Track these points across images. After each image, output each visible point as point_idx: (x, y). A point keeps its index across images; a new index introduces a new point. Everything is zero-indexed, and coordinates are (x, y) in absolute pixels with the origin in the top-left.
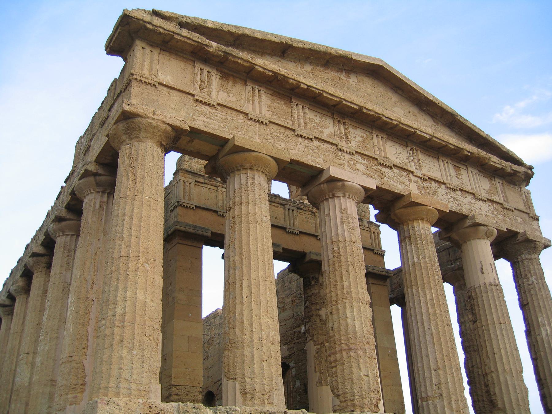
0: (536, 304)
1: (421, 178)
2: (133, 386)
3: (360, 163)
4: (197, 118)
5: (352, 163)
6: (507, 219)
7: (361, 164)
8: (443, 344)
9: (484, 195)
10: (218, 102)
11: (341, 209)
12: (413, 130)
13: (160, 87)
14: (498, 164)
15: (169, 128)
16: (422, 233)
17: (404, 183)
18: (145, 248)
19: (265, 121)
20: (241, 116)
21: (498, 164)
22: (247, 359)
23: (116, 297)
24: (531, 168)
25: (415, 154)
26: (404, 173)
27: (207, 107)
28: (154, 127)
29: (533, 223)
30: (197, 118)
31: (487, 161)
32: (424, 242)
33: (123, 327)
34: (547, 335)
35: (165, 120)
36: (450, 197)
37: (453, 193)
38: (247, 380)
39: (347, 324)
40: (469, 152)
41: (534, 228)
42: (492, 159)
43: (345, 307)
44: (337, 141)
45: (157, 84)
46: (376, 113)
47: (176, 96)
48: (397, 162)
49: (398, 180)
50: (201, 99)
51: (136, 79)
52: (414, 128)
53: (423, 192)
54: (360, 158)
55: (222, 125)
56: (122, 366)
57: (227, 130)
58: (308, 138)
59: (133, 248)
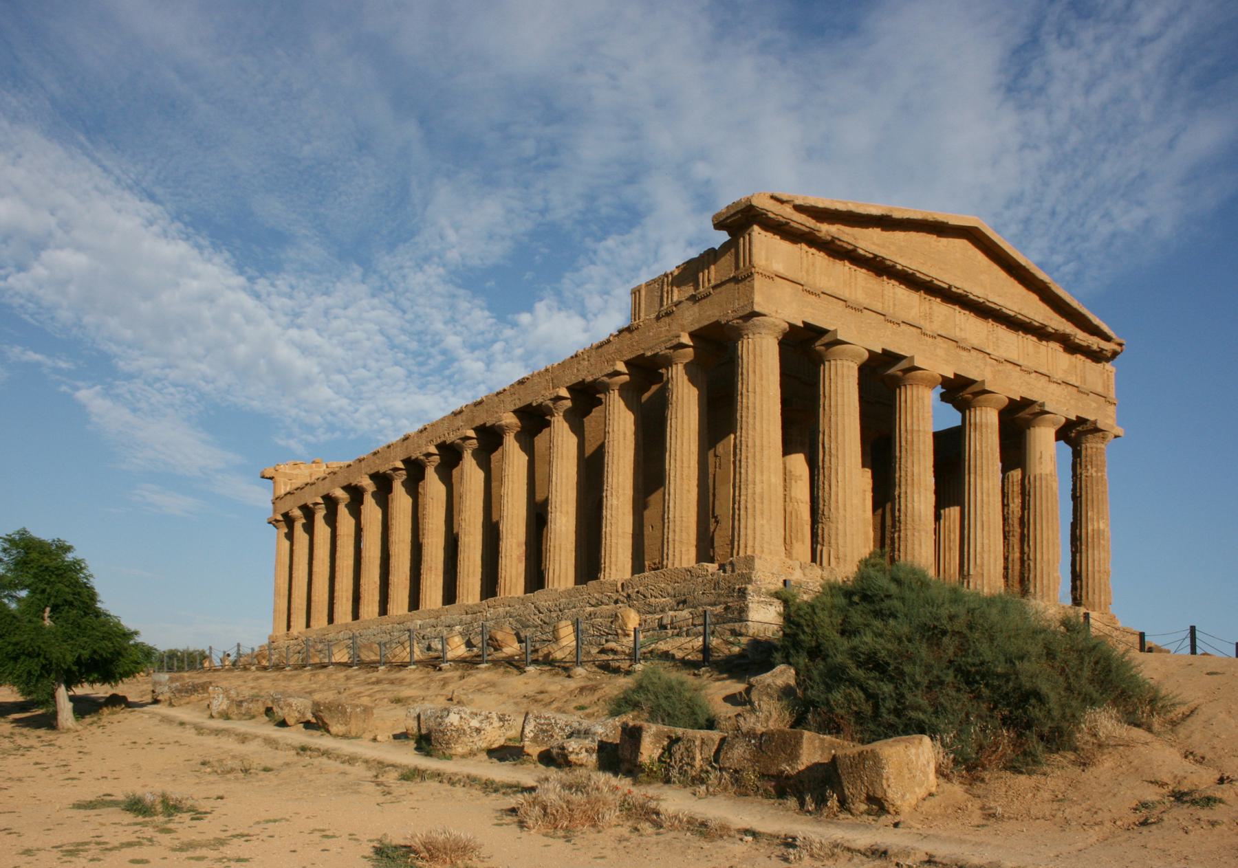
0: (1089, 497)
13: (776, 278)
16: (989, 421)
26: (981, 355)
27: (814, 297)
32: (989, 431)
34: (1093, 530)
37: (1026, 377)
39: (913, 507)
43: (913, 493)
44: (922, 323)
45: (773, 276)
48: (975, 342)
50: (809, 289)
54: (941, 341)
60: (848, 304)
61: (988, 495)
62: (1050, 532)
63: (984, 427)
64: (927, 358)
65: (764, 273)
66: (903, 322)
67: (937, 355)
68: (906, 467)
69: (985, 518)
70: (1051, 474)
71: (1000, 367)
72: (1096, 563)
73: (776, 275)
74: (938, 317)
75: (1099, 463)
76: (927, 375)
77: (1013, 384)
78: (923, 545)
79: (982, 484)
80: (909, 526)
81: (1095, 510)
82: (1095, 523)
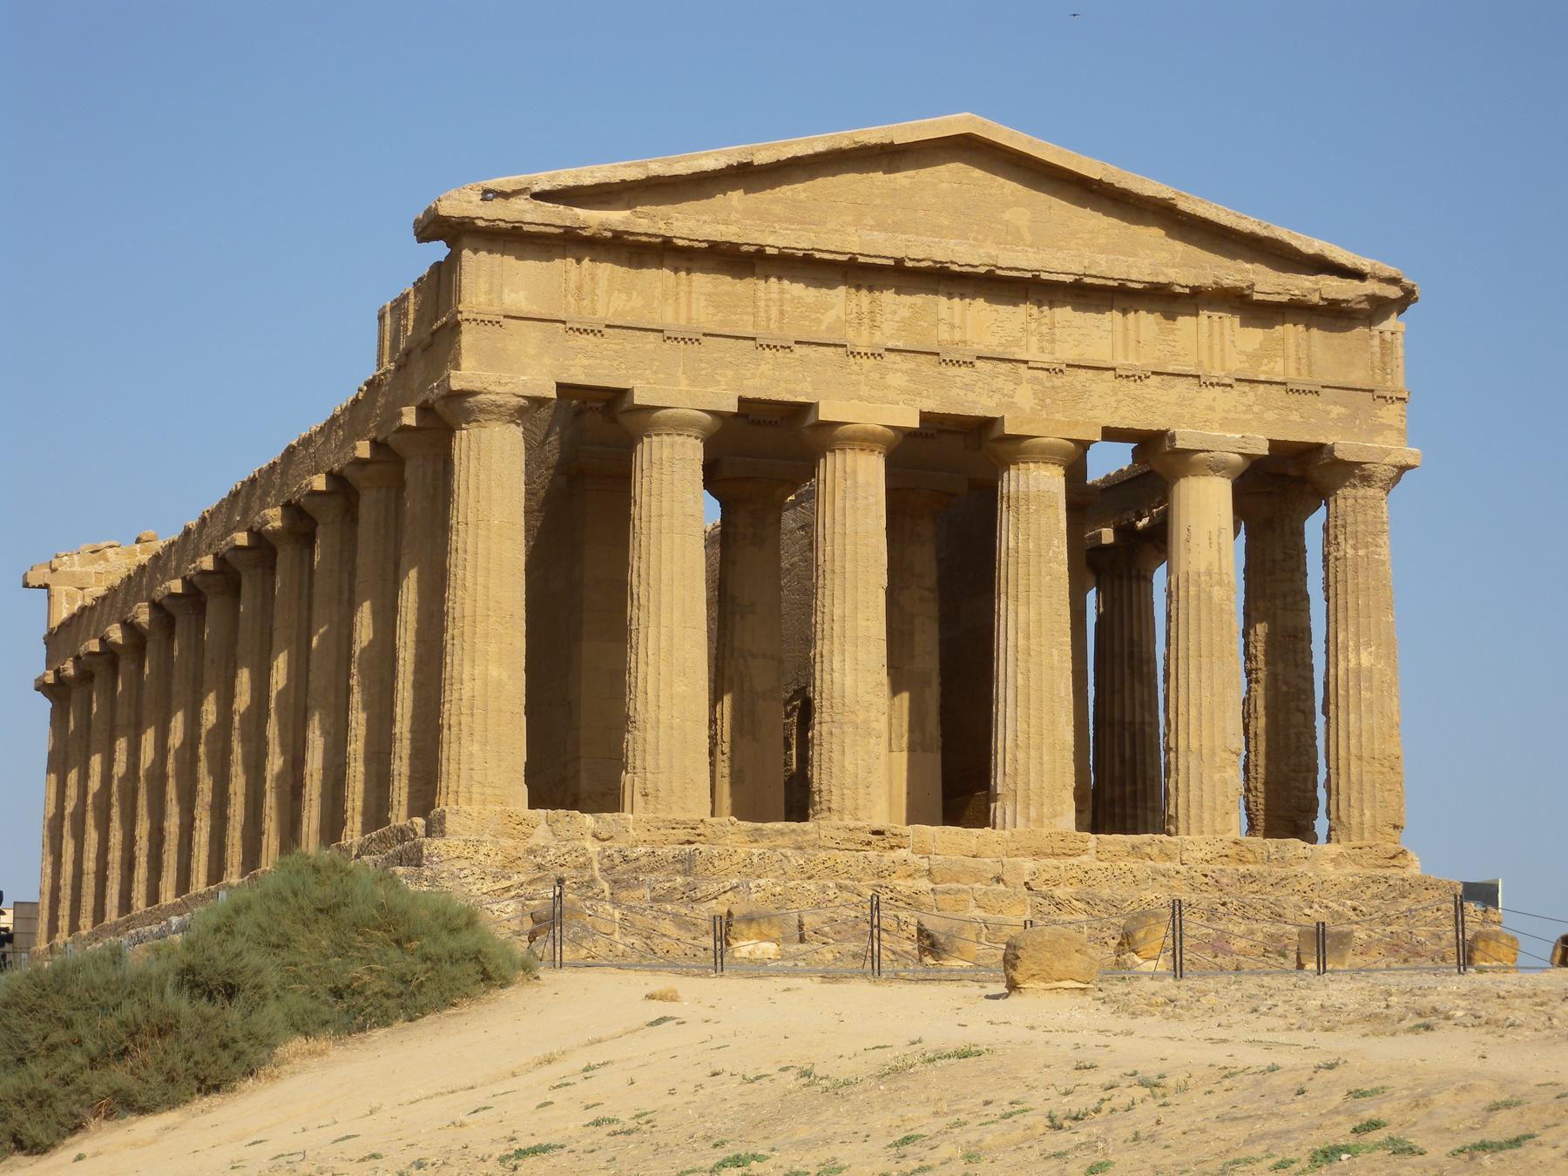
1: (1048, 370)
2: (488, 791)
3: (900, 371)
4: (571, 362)
5: (875, 375)
6: (1295, 417)
7: (898, 372)
8: (1033, 705)
10: (607, 323)
11: (845, 472)
12: (1029, 275)
14: (1279, 294)
15: (523, 401)
16: (1033, 489)
17: (999, 390)
18: (497, 602)
19: (694, 337)
20: (652, 335)
21: (1279, 294)
22: (650, 748)
23: (461, 673)
24: (1394, 281)
25: (1045, 313)
28: (501, 406)
29: (1379, 413)
30: (571, 362)
31: (1247, 292)
33: (472, 715)
35: (516, 391)
36: (1121, 396)
40: (1187, 286)
41: (1383, 425)
42: (1256, 288)
43: (832, 652)
47: (533, 332)
49: (986, 386)
50: (576, 326)
52: (1032, 271)
53: (1048, 401)
55: (616, 363)
56: (473, 767)
57: (624, 372)
58: (781, 347)
59: (480, 603)
60: (667, 334)
61: (1028, 638)
62: (1206, 693)
63: (1022, 502)
64: (860, 398)
65: (480, 317)
66: (797, 342)
67: (887, 387)
68: (824, 606)
69: (1020, 681)
70: (1209, 573)
71: (1058, 381)
72: (1353, 742)
75: (1361, 528)
76: (854, 432)
79: (1017, 613)
80: (826, 717)
81: (1352, 629)
82: (1352, 656)
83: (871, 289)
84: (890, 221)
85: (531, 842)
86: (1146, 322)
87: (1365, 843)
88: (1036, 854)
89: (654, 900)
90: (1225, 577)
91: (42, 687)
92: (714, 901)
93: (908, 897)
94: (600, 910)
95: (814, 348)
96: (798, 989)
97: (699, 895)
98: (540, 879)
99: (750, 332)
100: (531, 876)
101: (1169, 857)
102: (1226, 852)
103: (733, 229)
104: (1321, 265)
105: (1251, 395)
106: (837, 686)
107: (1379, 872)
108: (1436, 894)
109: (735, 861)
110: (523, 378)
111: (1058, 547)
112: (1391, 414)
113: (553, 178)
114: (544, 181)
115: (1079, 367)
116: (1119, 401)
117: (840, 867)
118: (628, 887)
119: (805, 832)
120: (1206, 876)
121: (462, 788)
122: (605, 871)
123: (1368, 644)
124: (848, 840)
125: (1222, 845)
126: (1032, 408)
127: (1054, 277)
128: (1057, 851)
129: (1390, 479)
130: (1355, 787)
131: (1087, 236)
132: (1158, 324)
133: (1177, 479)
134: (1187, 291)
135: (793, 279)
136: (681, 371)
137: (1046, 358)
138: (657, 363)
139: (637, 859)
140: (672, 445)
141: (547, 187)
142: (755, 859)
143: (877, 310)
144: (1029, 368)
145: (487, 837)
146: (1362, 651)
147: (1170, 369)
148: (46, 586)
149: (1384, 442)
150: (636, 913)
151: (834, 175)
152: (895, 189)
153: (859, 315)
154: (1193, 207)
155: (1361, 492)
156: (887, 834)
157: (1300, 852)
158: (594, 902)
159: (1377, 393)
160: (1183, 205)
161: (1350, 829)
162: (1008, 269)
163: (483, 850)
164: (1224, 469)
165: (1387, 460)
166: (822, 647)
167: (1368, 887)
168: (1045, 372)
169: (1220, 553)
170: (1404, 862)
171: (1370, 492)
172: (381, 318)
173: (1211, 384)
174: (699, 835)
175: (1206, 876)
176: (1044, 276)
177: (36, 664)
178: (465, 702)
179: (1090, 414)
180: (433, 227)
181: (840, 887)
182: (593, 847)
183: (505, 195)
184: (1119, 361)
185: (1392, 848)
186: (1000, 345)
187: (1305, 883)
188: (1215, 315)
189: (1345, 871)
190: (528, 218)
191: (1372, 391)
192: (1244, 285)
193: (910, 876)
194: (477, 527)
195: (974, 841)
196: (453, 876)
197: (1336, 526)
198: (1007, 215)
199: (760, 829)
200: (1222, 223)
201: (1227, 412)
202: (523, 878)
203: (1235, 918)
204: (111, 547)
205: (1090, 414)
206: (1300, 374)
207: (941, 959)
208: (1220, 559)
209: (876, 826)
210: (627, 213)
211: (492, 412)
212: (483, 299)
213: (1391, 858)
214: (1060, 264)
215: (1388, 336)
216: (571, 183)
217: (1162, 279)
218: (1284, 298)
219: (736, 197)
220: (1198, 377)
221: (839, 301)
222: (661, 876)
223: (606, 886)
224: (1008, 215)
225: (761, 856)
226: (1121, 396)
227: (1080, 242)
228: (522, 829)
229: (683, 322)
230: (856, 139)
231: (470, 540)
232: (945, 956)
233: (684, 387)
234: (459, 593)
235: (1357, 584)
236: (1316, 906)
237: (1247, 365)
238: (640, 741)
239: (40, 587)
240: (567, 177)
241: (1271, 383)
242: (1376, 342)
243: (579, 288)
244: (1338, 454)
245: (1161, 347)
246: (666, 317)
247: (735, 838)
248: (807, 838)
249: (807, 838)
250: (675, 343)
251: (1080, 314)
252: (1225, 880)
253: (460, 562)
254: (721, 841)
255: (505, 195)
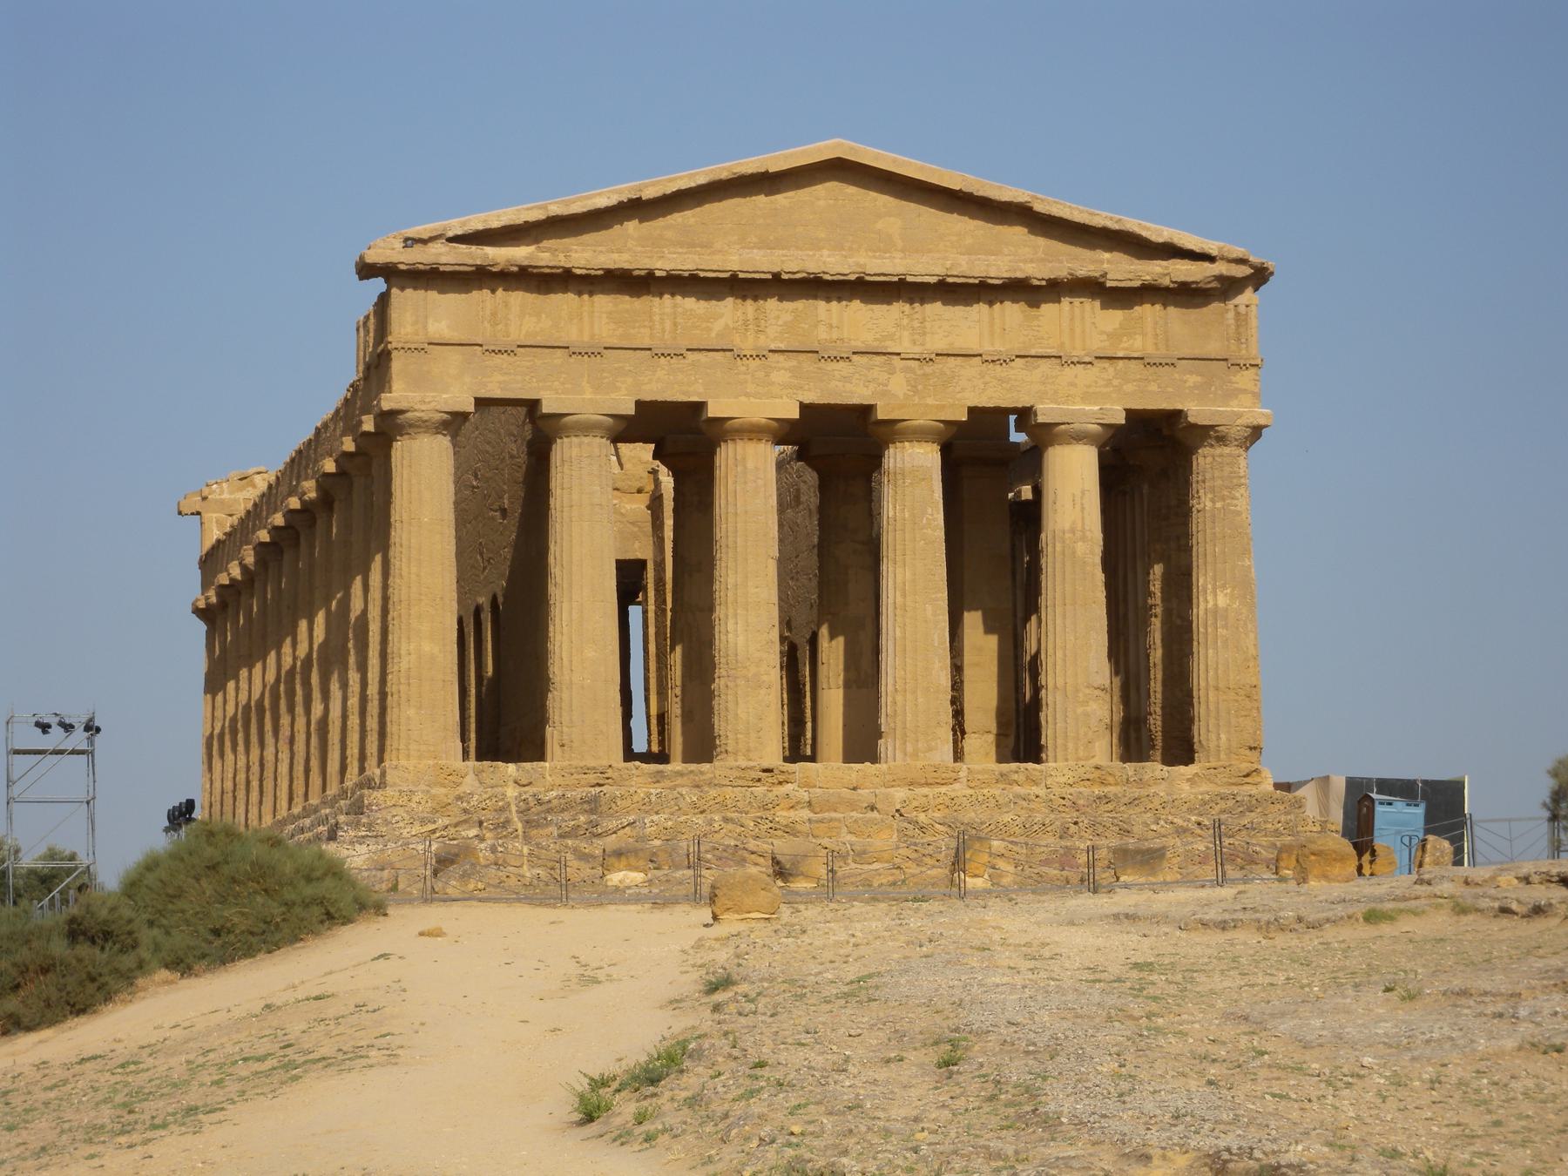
2: (423, 748)
3: (783, 368)
5: (761, 374)
6: (1153, 387)
7: (782, 371)
9: (1098, 344)
12: (896, 279)
15: (446, 416)
23: (399, 649)
24: (1242, 261)
28: (426, 421)
29: (1234, 379)
31: (1102, 280)
33: (409, 684)
35: (438, 408)
36: (987, 378)
38: (565, 729)
40: (1043, 279)
41: (1237, 389)
42: (1108, 277)
46: (808, 273)
47: (454, 355)
50: (492, 348)
51: (396, 349)
53: (920, 387)
60: (572, 350)
63: (899, 477)
64: (747, 395)
65: (407, 346)
66: (688, 350)
69: (898, 633)
70: (1073, 531)
71: (928, 369)
72: (1211, 673)
73: (429, 344)
74: (778, 317)
77: (963, 390)
78: (740, 701)
81: (1210, 574)
82: (1210, 598)
83: (755, 299)
84: (771, 238)
85: (460, 791)
86: (1011, 312)
87: (1221, 763)
88: (912, 784)
89: (560, 836)
90: (1088, 534)
91: (198, 612)
92: (614, 835)
93: (786, 826)
94: (510, 847)
95: (705, 353)
96: (561, 922)
97: (600, 831)
98: (465, 821)
99: (646, 343)
100: (458, 819)
101: (1036, 783)
102: (1086, 776)
103: (626, 256)
104: (1171, 251)
105: (1111, 370)
106: (731, 645)
107: (1225, 790)
108: (1282, 808)
109: (635, 800)
110: (444, 396)
111: (932, 515)
112: (1244, 379)
113: (464, 224)
114: (456, 227)
115: (948, 355)
116: (986, 383)
117: (728, 802)
118: (538, 826)
119: (702, 773)
120: (1064, 798)
121: (402, 747)
122: (521, 812)
123: (1224, 587)
124: (740, 778)
125: (1083, 770)
126: (905, 394)
127: (919, 279)
128: (930, 781)
129: (1246, 438)
130: (1213, 714)
131: (954, 238)
132: (1022, 312)
133: (1047, 447)
134: (1044, 283)
135: (684, 295)
136: (585, 379)
137: (917, 349)
138: (564, 376)
139: (550, 801)
140: (580, 445)
141: (460, 232)
142: (653, 798)
143: (761, 317)
144: (902, 359)
145: (423, 787)
146: (1219, 593)
147: (1033, 352)
148: (199, 513)
149: (1238, 406)
150: (542, 848)
151: (720, 201)
152: (776, 209)
153: (746, 323)
154: (1047, 208)
155: (1218, 451)
156: (776, 771)
157: (1158, 774)
158: (504, 840)
159: (1230, 362)
160: (1039, 207)
161: (1208, 751)
162: (875, 275)
163: (416, 799)
164: (1085, 438)
165: (1239, 422)
166: (720, 612)
167: (1217, 804)
168: (917, 362)
169: (1083, 512)
170: (1257, 779)
171: (1227, 450)
172: (358, 330)
173: (1072, 363)
174: (608, 778)
175: (1064, 798)
176: (910, 279)
177: (190, 588)
178: (403, 674)
179: (958, 396)
180: (367, 271)
181: (726, 820)
182: (512, 792)
183: (424, 242)
184: (986, 348)
185: (1245, 767)
186: (876, 340)
187: (1157, 802)
188: (1077, 301)
189: (1201, 789)
190: (443, 260)
191: (1226, 360)
192: (1097, 275)
193: (792, 807)
194: (410, 524)
195: (854, 775)
196: (387, 823)
197: (1198, 482)
198: (879, 225)
199: (662, 772)
200: (1076, 220)
201: (1090, 386)
202: (447, 821)
203: (1086, 835)
204: (259, 473)
205: (958, 396)
206: (1157, 349)
207: (788, 881)
208: (1083, 518)
209: (766, 765)
210: (532, 249)
211: (419, 427)
212: (409, 329)
213: (1244, 776)
214: (924, 268)
215: (1242, 309)
216: (480, 227)
217: (1019, 275)
218: (1137, 284)
219: (632, 226)
220: (1060, 357)
221: (728, 311)
222: (566, 815)
223: (520, 826)
224: (879, 225)
225: (659, 795)
226: (987, 378)
227: (948, 244)
228: (454, 777)
229: (586, 338)
230: (735, 171)
231: (405, 536)
232: (791, 879)
233: (588, 396)
234: (398, 581)
235: (1214, 533)
236: (1162, 822)
237: (1107, 343)
238: (557, 699)
239: (192, 514)
240: (476, 223)
241: (1129, 358)
242: (1231, 315)
243: (494, 314)
244: (1191, 419)
245: (1026, 333)
246: (572, 334)
247: (640, 780)
248: (704, 777)
249: (702, 778)
250: (580, 357)
251: (950, 308)
252: (1081, 802)
253: (397, 555)
254: (627, 783)
255: (424, 242)
